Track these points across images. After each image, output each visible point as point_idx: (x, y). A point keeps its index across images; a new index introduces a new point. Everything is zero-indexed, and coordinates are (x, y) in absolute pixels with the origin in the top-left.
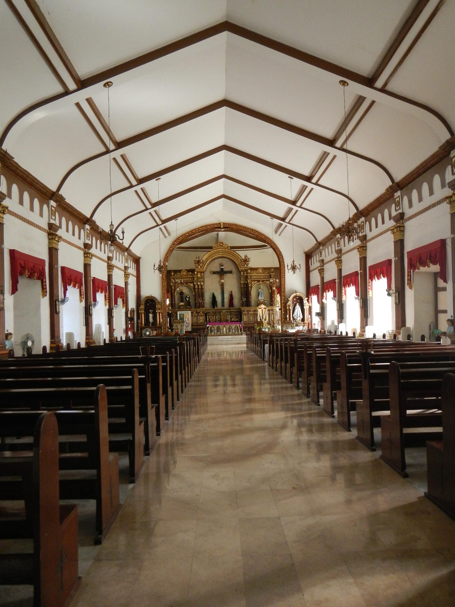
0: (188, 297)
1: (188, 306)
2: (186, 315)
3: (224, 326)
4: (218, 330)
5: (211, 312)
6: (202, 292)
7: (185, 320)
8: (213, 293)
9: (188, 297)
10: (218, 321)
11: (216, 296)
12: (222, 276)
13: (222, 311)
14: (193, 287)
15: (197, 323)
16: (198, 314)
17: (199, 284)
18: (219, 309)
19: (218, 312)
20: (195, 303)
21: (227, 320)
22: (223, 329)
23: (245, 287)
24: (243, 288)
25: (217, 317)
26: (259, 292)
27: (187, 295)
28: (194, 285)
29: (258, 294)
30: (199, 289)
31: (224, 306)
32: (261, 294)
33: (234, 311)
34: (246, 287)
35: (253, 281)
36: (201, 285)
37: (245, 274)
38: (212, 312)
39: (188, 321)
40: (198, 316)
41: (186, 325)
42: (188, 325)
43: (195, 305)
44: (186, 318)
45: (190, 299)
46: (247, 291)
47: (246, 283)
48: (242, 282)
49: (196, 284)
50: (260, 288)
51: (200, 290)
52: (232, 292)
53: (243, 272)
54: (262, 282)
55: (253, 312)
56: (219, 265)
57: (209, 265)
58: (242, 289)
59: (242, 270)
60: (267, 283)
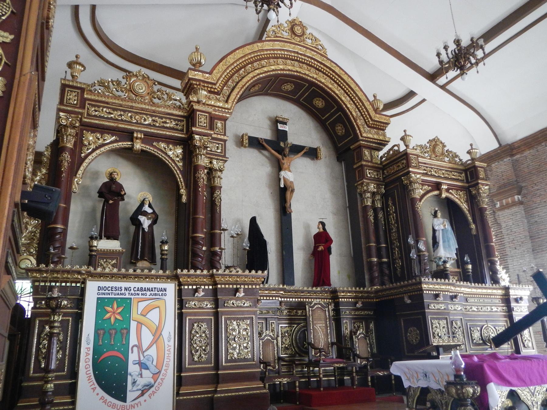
0: (145, 214)
2: (142, 305)
7: (133, 341)
8: (253, 221)
9: (145, 214)
12: (285, 156)
13: (311, 303)
27: (142, 204)
31: (293, 284)
39: (153, 352)
41: (141, 382)
42: (156, 375)
44: (144, 329)
45: (155, 227)
52: (323, 224)
59: (368, 139)
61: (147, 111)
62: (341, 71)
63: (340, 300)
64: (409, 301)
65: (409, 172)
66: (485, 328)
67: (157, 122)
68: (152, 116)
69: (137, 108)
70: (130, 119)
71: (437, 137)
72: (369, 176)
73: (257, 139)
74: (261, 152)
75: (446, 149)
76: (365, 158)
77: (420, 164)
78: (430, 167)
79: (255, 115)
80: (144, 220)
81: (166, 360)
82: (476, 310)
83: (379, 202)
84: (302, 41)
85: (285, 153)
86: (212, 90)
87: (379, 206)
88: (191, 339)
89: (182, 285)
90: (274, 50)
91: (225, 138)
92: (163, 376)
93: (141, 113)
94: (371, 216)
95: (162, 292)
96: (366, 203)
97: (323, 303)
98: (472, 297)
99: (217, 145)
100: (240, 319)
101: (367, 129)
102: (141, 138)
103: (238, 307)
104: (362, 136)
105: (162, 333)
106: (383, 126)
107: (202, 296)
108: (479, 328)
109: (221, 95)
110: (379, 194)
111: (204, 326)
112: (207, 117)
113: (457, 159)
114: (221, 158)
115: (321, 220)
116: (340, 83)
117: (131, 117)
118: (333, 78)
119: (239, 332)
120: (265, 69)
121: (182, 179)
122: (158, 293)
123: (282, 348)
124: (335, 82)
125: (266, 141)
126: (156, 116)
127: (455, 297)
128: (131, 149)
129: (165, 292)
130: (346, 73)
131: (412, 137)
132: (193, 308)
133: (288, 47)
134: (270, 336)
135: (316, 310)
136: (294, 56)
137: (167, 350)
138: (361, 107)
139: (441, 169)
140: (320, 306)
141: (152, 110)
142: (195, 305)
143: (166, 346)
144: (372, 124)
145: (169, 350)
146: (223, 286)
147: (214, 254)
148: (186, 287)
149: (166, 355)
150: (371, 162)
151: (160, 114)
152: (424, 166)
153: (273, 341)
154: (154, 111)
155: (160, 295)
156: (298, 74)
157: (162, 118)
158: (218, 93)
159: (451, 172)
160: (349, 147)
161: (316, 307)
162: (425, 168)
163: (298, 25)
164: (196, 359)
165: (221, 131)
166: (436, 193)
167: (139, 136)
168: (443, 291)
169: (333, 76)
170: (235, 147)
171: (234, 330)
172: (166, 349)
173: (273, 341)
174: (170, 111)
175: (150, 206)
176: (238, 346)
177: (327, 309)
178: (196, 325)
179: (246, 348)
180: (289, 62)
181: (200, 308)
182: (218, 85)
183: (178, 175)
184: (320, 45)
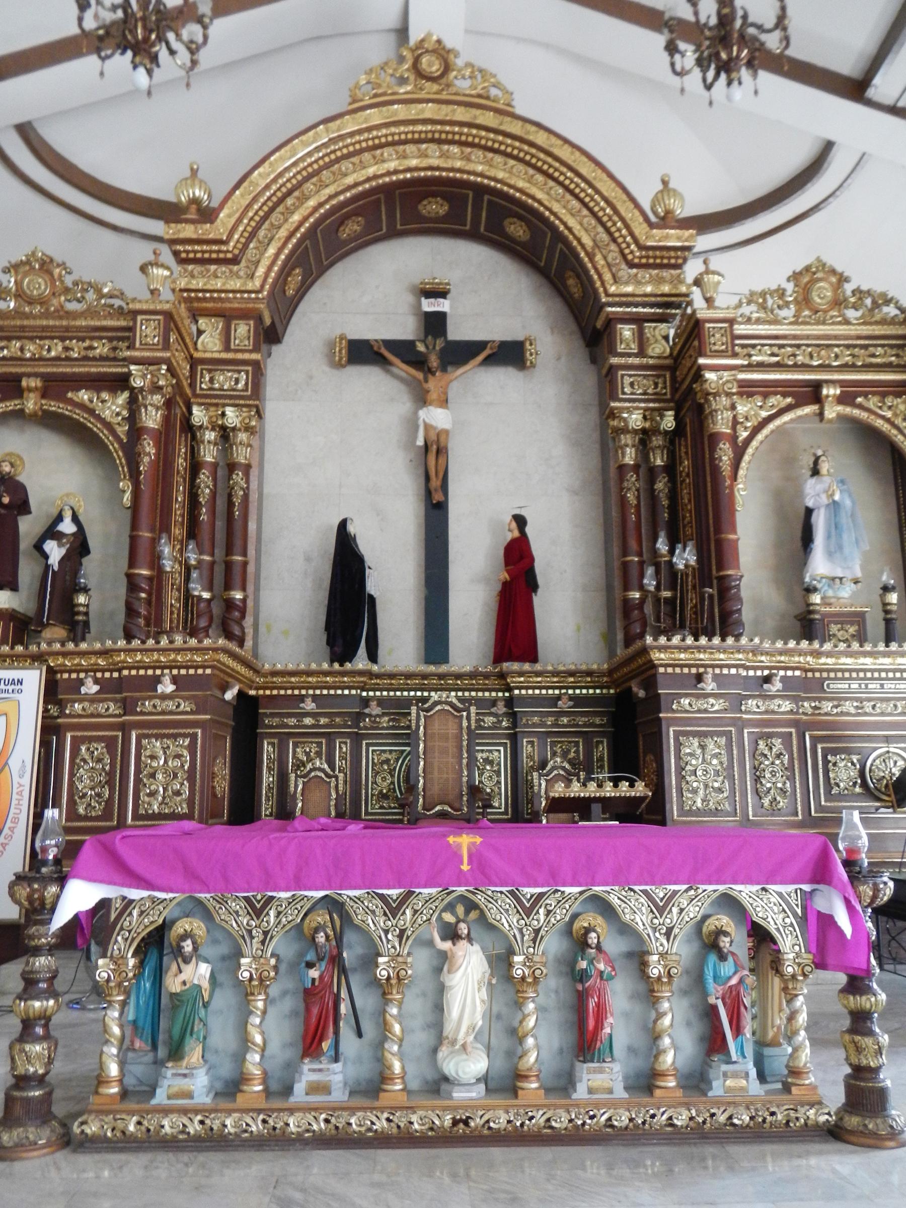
1: (48, 624)
3: (462, 898)
4: (310, 994)
5: (309, 706)
6: (230, 504)
8: (343, 525)
10: (383, 796)
11: (364, 547)
12: (431, 371)
13: (424, 700)
14: (122, 430)
15: (107, 815)
16: (128, 707)
17: (199, 415)
18: (392, 676)
19: (381, 702)
20: (132, 584)
21: (475, 791)
22: (441, 989)
23: (652, 473)
24: (636, 468)
25: (370, 754)
26: (809, 512)
27: (59, 518)
28: (133, 405)
29: (798, 533)
30: (195, 467)
31: (445, 659)
32: (835, 528)
33: (559, 698)
34: (670, 469)
35: (748, 390)
36: (225, 434)
37: (659, 349)
38: (315, 698)
40: (125, 728)
43: (131, 611)
46: (673, 507)
47: (669, 422)
48: (635, 420)
49: (156, 389)
50: (815, 472)
51: (204, 478)
52: (520, 521)
53: (639, 321)
54: (842, 400)
55: (787, 706)
56: (410, 298)
57: (316, 293)
58: (632, 477)
59: (626, 300)
60: (883, 417)
61: (52, 331)
62: (554, 140)
63: (517, 692)
64: (642, 694)
65: (700, 368)
66: (879, 756)
67: (73, 350)
68: (63, 339)
69: (33, 328)
70: (19, 353)
71: (818, 259)
72: (627, 390)
73: (366, 343)
74: (388, 371)
75: (849, 288)
76: (621, 348)
77: (737, 342)
78: (791, 346)
79: (377, 287)
80: (52, 550)
81: (12, 810)
82: (853, 711)
83: (658, 452)
84: (443, 90)
85: (430, 365)
86: (221, 256)
87: (659, 462)
88: (72, 775)
89: (56, 672)
90: (369, 129)
91: (255, 356)
92: (5, 838)
93: (41, 338)
94: (629, 489)
95: (13, 687)
96: (620, 458)
97: (455, 701)
98: (843, 679)
99: (236, 376)
100: (168, 736)
101: (625, 272)
102: (36, 388)
103: (163, 713)
104: (607, 295)
105: (10, 762)
106: (677, 258)
107: (97, 693)
108: (855, 758)
109: (243, 263)
110: (660, 433)
111: (99, 748)
112: (159, 324)
113: (891, 311)
114: (242, 402)
115: (517, 512)
116: (551, 171)
117: (22, 349)
118: (534, 161)
119: (166, 762)
120: (349, 180)
121: (123, 460)
122: (7, 688)
123: (372, 795)
124: (540, 170)
125: (389, 344)
126: (71, 339)
127: (767, 680)
128: (22, 411)
129: (19, 687)
130: (566, 141)
131: (722, 276)
132: (80, 716)
133: (413, 112)
134: (323, 771)
135: (436, 717)
136: (426, 132)
137: (17, 793)
138: (610, 219)
139: (828, 346)
140: (447, 708)
141: (62, 327)
142: (84, 709)
143: (15, 785)
144: (641, 257)
145: (20, 793)
146: (134, 672)
147: (229, 604)
148: (66, 676)
149: (14, 802)
150: (641, 353)
151: (80, 332)
152: (771, 345)
153: (328, 780)
154: (67, 329)
155: (10, 691)
156: (374, 183)
157: (83, 339)
158: (235, 261)
159: (865, 347)
160: (595, 327)
161: (439, 707)
162: (775, 350)
163: (434, 51)
164: (81, 811)
165: (246, 343)
166: (808, 410)
167: (33, 384)
168: (713, 666)
169: (533, 156)
170: (327, 369)
171: (153, 757)
172: (15, 791)
173: (328, 780)
174: (97, 323)
175: (75, 519)
176: (161, 789)
177: (465, 714)
178: (83, 748)
179: (178, 793)
180: (410, 148)
181: (92, 716)
182: (232, 244)
183: (117, 452)
184: (494, 86)
